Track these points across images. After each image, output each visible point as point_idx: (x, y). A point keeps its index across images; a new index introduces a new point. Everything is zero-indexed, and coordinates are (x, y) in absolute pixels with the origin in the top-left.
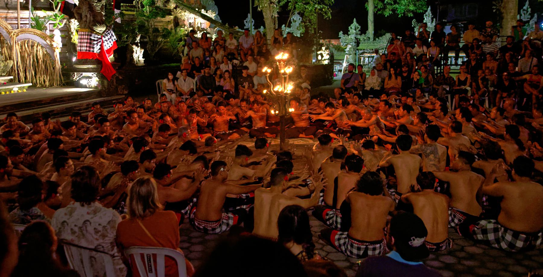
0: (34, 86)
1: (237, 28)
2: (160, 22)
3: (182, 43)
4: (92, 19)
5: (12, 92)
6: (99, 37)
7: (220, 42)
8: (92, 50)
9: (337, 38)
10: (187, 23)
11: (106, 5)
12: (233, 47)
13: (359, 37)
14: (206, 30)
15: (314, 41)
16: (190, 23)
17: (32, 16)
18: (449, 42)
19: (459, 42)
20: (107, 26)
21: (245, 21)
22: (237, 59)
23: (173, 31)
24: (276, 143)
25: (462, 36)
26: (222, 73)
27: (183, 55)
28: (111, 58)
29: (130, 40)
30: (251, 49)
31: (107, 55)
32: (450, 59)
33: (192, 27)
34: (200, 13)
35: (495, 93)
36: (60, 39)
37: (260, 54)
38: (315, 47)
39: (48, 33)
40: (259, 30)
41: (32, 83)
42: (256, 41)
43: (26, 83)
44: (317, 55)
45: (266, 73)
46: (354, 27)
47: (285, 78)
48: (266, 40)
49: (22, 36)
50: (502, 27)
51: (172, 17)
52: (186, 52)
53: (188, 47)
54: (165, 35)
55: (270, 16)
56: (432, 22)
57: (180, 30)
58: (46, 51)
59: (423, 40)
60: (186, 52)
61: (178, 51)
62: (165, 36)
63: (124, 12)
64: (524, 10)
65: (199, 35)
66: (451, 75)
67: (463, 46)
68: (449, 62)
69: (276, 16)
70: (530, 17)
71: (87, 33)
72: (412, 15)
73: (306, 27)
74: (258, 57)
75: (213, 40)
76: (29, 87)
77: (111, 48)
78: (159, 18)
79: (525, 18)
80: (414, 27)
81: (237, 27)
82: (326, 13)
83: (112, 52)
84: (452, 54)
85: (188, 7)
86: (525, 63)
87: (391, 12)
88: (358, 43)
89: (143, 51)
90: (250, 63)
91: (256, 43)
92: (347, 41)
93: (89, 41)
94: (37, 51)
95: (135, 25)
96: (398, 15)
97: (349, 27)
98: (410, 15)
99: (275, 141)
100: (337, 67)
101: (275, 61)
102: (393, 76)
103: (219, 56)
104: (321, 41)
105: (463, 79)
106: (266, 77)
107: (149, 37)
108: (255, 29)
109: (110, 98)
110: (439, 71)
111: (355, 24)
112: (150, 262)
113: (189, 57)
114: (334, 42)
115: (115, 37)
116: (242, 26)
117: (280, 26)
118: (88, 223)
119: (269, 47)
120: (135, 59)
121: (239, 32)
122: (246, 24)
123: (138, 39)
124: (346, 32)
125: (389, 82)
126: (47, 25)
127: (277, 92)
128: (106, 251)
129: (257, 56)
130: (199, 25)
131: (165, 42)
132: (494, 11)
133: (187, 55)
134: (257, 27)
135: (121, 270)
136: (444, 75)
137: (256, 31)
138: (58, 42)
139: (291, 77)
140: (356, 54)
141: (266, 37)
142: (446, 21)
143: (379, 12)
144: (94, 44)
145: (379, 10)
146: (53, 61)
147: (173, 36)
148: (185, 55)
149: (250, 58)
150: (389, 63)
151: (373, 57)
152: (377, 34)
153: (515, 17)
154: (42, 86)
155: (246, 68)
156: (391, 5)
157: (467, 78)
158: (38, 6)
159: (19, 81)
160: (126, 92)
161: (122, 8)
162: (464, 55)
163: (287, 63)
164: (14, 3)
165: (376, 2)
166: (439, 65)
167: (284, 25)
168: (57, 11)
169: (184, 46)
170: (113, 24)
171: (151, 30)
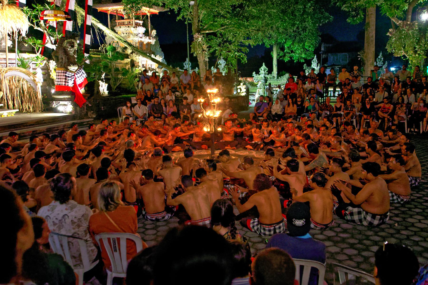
0: (21, 111)
1: (178, 68)
2: (120, 63)
3: (137, 79)
4: (67, 60)
5: (3, 116)
6: (73, 74)
7: (166, 78)
8: (67, 84)
9: (251, 76)
10: (140, 64)
11: (77, 51)
12: (175, 83)
13: (267, 76)
15: (234, 79)
16: (143, 65)
17: (18, 57)
18: (329, 80)
19: (336, 80)
20: (79, 66)
21: (184, 64)
22: (178, 92)
23: (130, 70)
24: (208, 153)
25: (338, 76)
26: (167, 103)
28: (82, 91)
29: (97, 77)
30: (189, 84)
31: (79, 88)
32: (329, 92)
34: (150, 57)
35: (360, 116)
36: (42, 76)
37: (196, 87)
39: (31, 71)
40: (195, 70)
41: (19, 109)
42: (192, 78)
43: (14, 109)
44: (237, 89)
45: (200, 102)
46: (263, 68)
47: (214, 106)
48: (200, 78)
49: (10, 73)
50: (364, 71)
51: (129, 60)
52: (140, 85)
53: (142, 82)
54: (124, 73)
55: (202, 60)
56: (317, 66)
58: (30, 84)
59: (313, 79)
60: (140, 85)
62: (124, 74)
63: (92, 55)
64: (379, 59)
65: (150, 74)
66: (331, 104)
67: (339, 83)
68: (329, 94)
69: (207, 60)
70: (383, 63)
71: (63, 71)
72: (304, 61)
73: (229, 69)
74: (195, 90)
75: (161, 77)
76: (17, 112)
77: (82, 83)
78: (119, 61)
79: (379, 64)
80: (305, 69)
81: (178, 68)
82: (243, 59)
83: (83, 85)
84: (331, 89)
85: (141, 53)
86: (380, 96)
87: (289, 59)
88: (266, 80)
89: (107, 85)
90: (189, 94)
91: (192, 79)
92: (258, 78)
93: (64, 77)
94: (22, 85)
95: (100, 65)
96: (294, 60)
98: (303, 61)
99: (207, 152)
100: (251, 98)
101: (207, 94)
102: (291, 104)
103: (165, 89)
105: (338, 106)
106: (200, 105)
107: (112, 75)
108: (192, 69)
109: (82, 121)
110: (322, 101)
111: (264, 67)
112: (115, 244)
113: (142, 90)
114: (249, 79)
115: (85, 75)
116: (182, 67)
117: (210, 68)
118: (66, 216)
119: (202, 83)
120: (101, 92)
121: (179, 71)
122: (185, 66)
123: (103, 76)
124: (258, 73)
125: (288, 108)
126: (31, 65)
128: (80, 237)
129: (194, 89)
132: (359, 59)
133: (141, 88)
134: (193, 68)
135: (92, 251)
136: (326, 104)
137: (192, 71)
138: (40, 78)
139: (219, 106)
140: (264, 88)
141: (200, 76)
142: (327, 65)
143: (281, 59)
144: (68, 80)
145: (281, 57)
146: (36, 93)
149: (187, 91)
150: (289, 94)
151: (277, 91)
152: (280, 75)
153: (373, 64)
154: (27, 112)
155: (186, 98)
156: (289, 53)
157: (341, 106)
158: (23, 50)
159: (8, 108)
160: (94, 116)
161: (90, 53)
162: (339, 89)
163: (216, 95)
164: (3, 47)
165: (279, 51)
166: (322, 97)
167: (213, 67)
168: (38, 54)
169: (138, 81)
170: (83, 64)
171: (113, 70)
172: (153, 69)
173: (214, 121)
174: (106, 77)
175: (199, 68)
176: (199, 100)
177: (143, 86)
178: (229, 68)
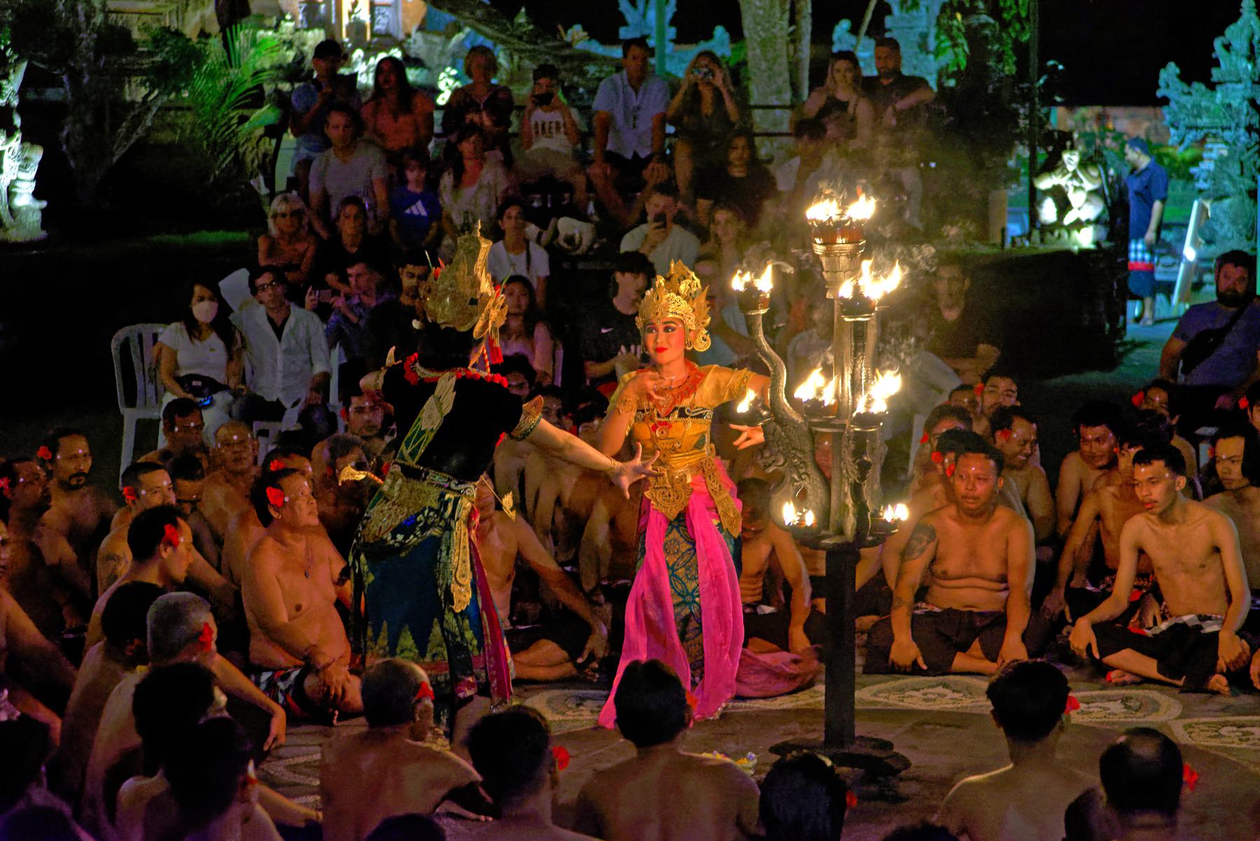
3: (266, 114)
7: (484, 110)
14: (400, 45)
15: (1015, 115)
22: (584, 218)
23: (215, 44)
27: (270, 183)
33: (323, 23)
38: (1023, 151)
44: (1035, 198)
47: (859, 332)
52: (284, 169)
54: (165, 62)
57: (254, 43)
60: (284, 169)
61: (239, 161)
62: (165, 76)
65: (363, 69)
74: (703, 204)
75: (442, 100)
89: (37, 155)
97: (1218, 43)
101: (805, 234)
103: (472, 195)
104: (1059, 118)
106: (750, 324)
107: (75, 76)
113: (305, 196)
119: (764, 148)
121: (587, 58)
124: (1199, 70)
127: (815, 407)
130: (364, 15)
131: (165, 109)
133: (292, 183)
137: (692, 51)
147: (212, 75)
148: (281, 184)
163: (868, 241)
167: (845, 24)
169: (274, 131)
171: (87, 39)
172: (386, 40)
173: (858, 452)
174: (31, 96)
175: (736, 34)
176: (738, 283)
177: (304, 165)
178: (973, 35)
